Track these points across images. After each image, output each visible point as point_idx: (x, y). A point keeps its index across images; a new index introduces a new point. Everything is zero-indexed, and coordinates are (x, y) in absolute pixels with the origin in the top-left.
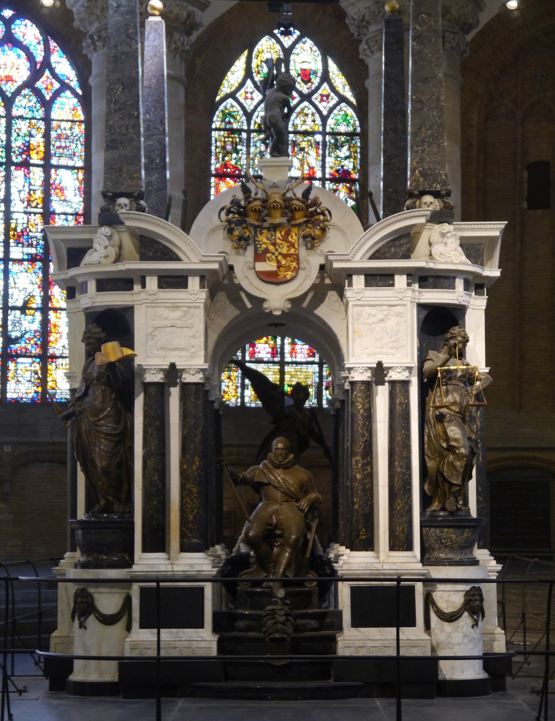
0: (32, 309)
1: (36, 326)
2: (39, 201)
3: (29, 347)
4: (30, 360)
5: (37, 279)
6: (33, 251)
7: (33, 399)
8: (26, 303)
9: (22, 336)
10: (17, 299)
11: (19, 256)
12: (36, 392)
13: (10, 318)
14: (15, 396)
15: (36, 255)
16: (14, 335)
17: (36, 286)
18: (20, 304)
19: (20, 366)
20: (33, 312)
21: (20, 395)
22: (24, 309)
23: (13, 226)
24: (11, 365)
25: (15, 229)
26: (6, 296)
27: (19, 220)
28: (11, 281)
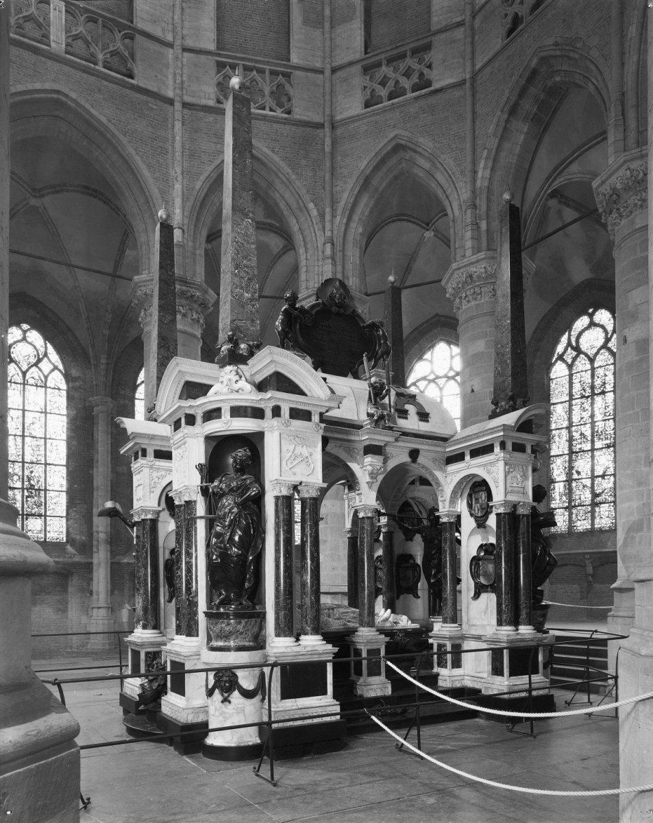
0: (608, 475)
1: (611, 485)
2: (611, 412)
3: (607, 497)
4: (608, 505)
5: (611, 458)
6: (608, 442)
7: (610, 527)
8: (605, 472)
9: (603, 492)
10: (599, 471)
11: (601, 446)
12: (612, 523)
13: (596, 482)
14: (599, 526)
15: (610, 444)
16: (598, 492)
17: (610, 462)
18: (601, 473)
19: (602, 509)
20: (608, 477)
21: (603, 525)
22: (603, 476)
23: (596, 430)
24: (597, 509)
25: (597, 432)
26: (593, 471)
27: (600, 426)
28: (596, 461)
